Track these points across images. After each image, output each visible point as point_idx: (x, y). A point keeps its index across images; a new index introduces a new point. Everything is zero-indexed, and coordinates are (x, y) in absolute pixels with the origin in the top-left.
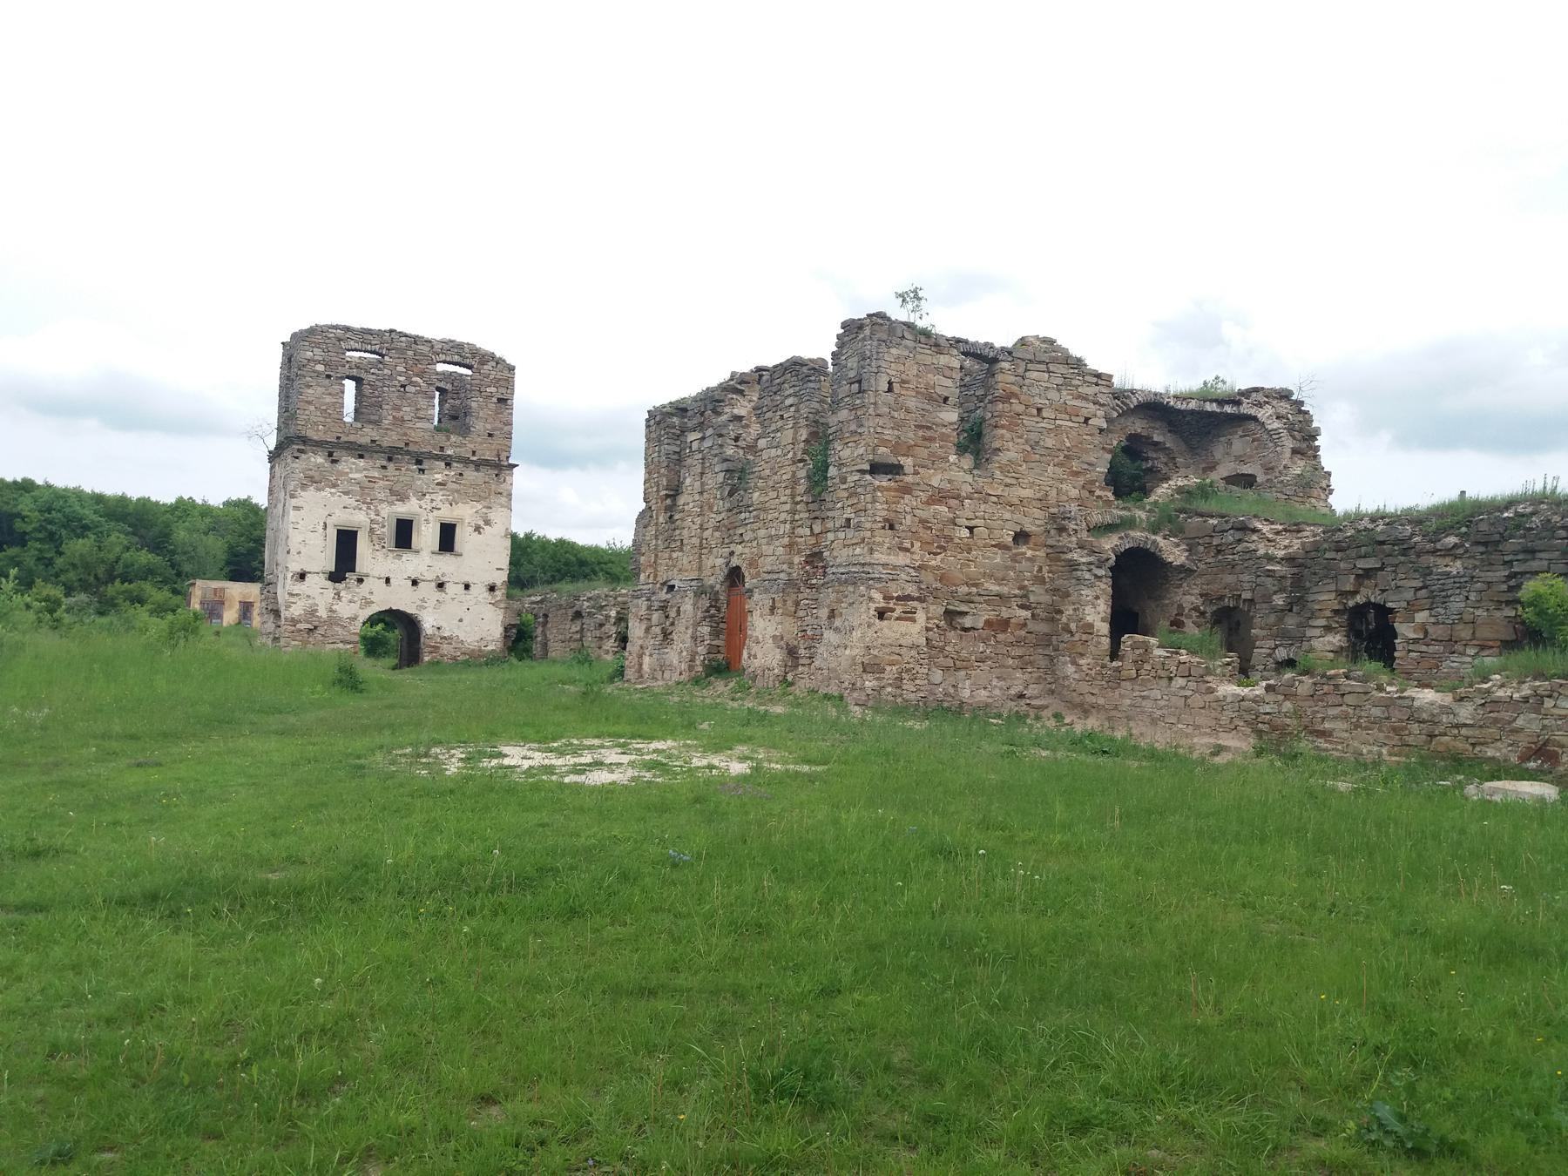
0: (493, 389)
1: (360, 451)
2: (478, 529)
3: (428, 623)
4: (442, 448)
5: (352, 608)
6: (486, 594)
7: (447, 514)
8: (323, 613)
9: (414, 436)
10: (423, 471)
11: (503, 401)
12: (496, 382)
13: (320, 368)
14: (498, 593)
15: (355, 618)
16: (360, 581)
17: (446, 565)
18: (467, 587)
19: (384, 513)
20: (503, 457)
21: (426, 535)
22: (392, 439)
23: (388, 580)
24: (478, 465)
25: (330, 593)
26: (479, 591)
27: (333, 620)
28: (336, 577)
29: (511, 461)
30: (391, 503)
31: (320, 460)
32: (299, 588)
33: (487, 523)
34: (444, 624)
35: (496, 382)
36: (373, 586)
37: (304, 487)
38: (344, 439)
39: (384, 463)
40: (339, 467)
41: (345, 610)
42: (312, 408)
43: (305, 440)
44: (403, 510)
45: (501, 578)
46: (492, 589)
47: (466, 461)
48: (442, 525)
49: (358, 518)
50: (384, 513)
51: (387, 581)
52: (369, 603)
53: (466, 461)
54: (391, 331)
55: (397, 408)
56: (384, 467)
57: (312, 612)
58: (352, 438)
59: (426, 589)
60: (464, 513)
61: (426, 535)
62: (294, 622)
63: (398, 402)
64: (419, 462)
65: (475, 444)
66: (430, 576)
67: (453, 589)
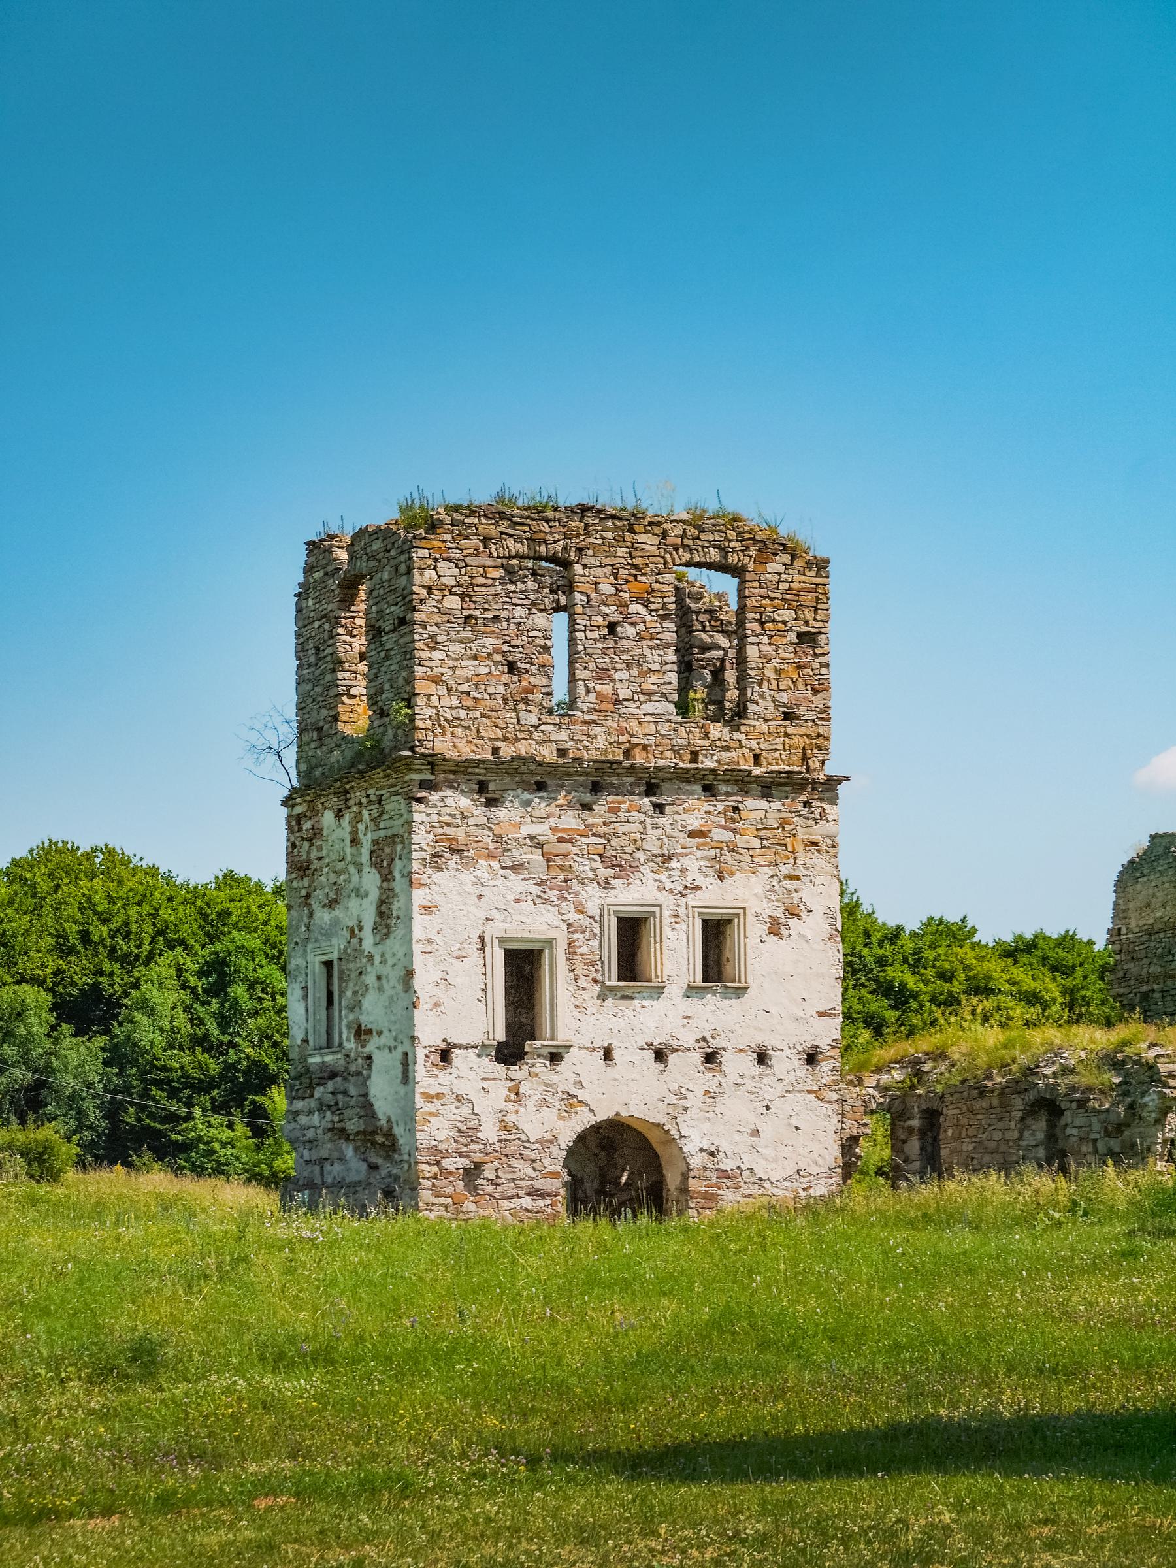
0: (787, 614)
1: (538, 779)
2: (775, 929)
3: (694, 1137)
4: (694, 756)
5: (544, 1117)
6: (802, 1071)
7: (716, 897)
8: (490, 1132)
9: (642, 732)
10: (659, 808)
11: (808, 639)
12: (794, 600)
13: (452, 602)
14: (825, 1066)
15: (547, 1143)
16: (555, 1057)
17: (715, 1015)
18: (762, 1058)
19: (593, 909)
20: (814, 764)
21: (676, 952)
22: (597, 743)
23: (608, 1054)
24: (769, 787)
25: (500, 1090)
26: (787, 1065)
27: (512, 1144)
28: (509, 1053)
29: (831, 769)
30: (607, 885)
31: (465, 802)
32: (445, 1080)
33: (792, 912)
34: (725, 1147)
35: (794, 600)
36: (580, 1065)
37: (436, 862)
38: (507, 751)
39: (587, 797)
40: (501, 813)
41: (534, 1122)
42: (442, 690)
43: (433, 762)
44: (634, 894)
45: (828, 1033)
46: (812, 1059)
47: (743, 782)
48: (705, 922)
49: (537, 922)
50: (593, 909)
51: (616, 1057)
52: (573, 1102)
53: (743, 782)
54: (584, 510)
55: (602, 675)
56: (587, 807)
57: (468, 1135)
58: (523, 748)
59: (685, 1067)
60: (747, 892)
61: (676, 952)
62: (437, 1155)
63: (605, 662)
64: (651, 789)
65: (764, 742)
66: (688, 1038)
67: (736, 1064)
